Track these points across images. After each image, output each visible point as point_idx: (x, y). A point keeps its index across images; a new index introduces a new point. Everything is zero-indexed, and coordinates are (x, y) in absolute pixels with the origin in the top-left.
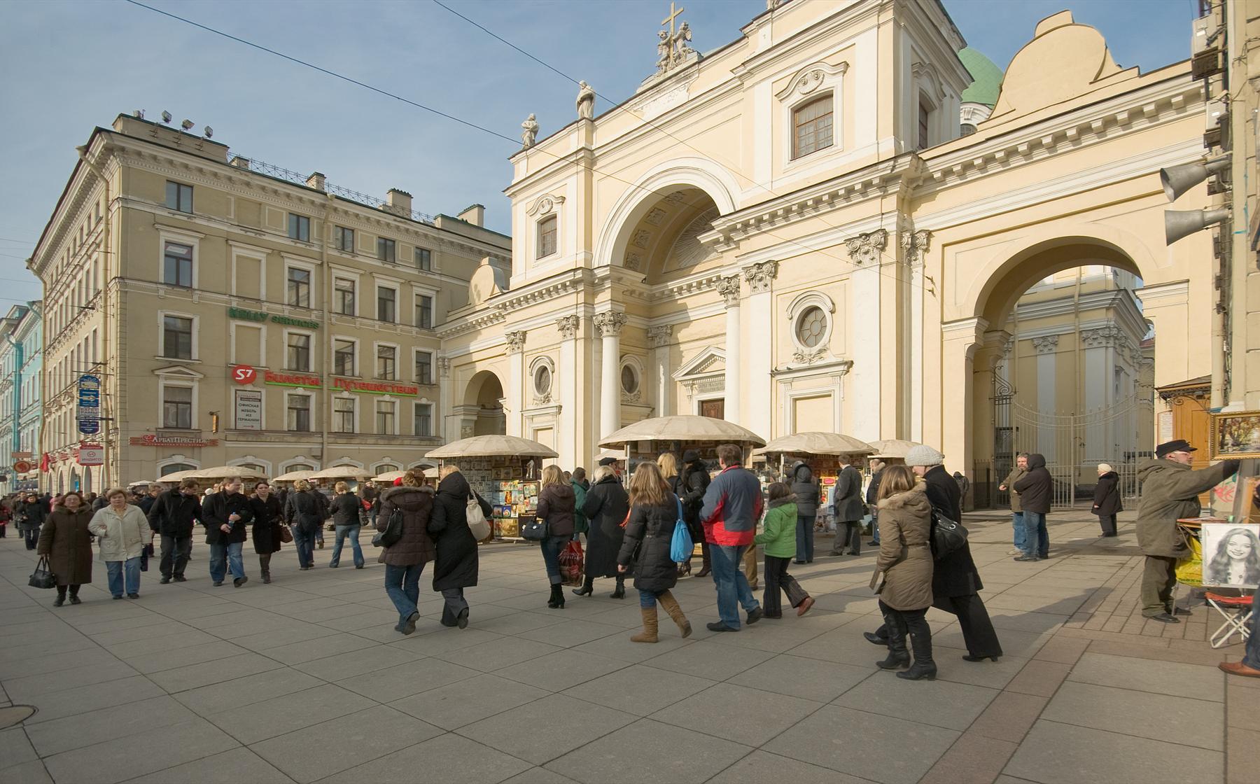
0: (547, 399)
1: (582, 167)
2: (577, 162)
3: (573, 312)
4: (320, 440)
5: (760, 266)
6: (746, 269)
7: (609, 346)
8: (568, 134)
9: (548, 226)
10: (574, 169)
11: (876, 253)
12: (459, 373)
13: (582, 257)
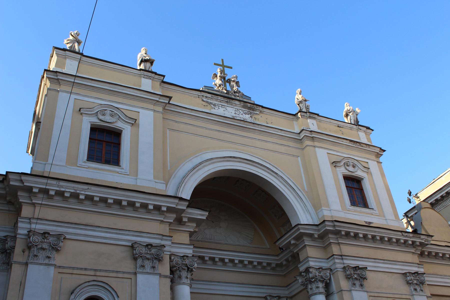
10: (151, 107)
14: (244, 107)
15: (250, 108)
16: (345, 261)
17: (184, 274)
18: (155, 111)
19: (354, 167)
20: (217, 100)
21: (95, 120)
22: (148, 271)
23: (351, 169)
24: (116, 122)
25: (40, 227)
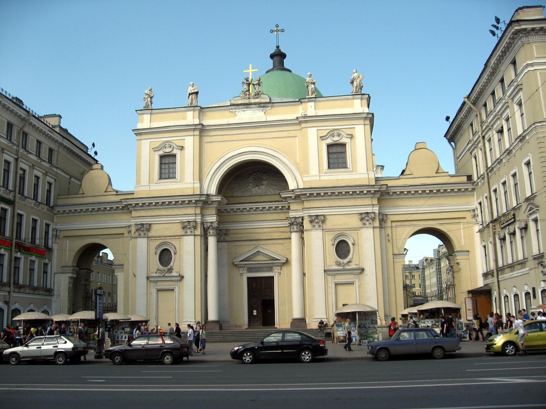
0: (170, 270)
1: (197, 133)
2: (194, 130)
3: (194, 218)
4: (7, 289)
5: (317, 216)
6: (310, 216)
7: (212, 241)
8: (186, 111)
9: (167, 160)
10: (191, 133)
11: (371, 221)
12: (67, 242)
13: (198, 185)
14: (259, 107)
15: (264, 107)
16: (311, 212)
17: (211, 231)
18: (194, 135)
19: (339, 135)
20: (239, 109)
21: (161, 153)
22: (189, 233)
23: (336, 138)
24: (172, 150)
25: (140, 221)
